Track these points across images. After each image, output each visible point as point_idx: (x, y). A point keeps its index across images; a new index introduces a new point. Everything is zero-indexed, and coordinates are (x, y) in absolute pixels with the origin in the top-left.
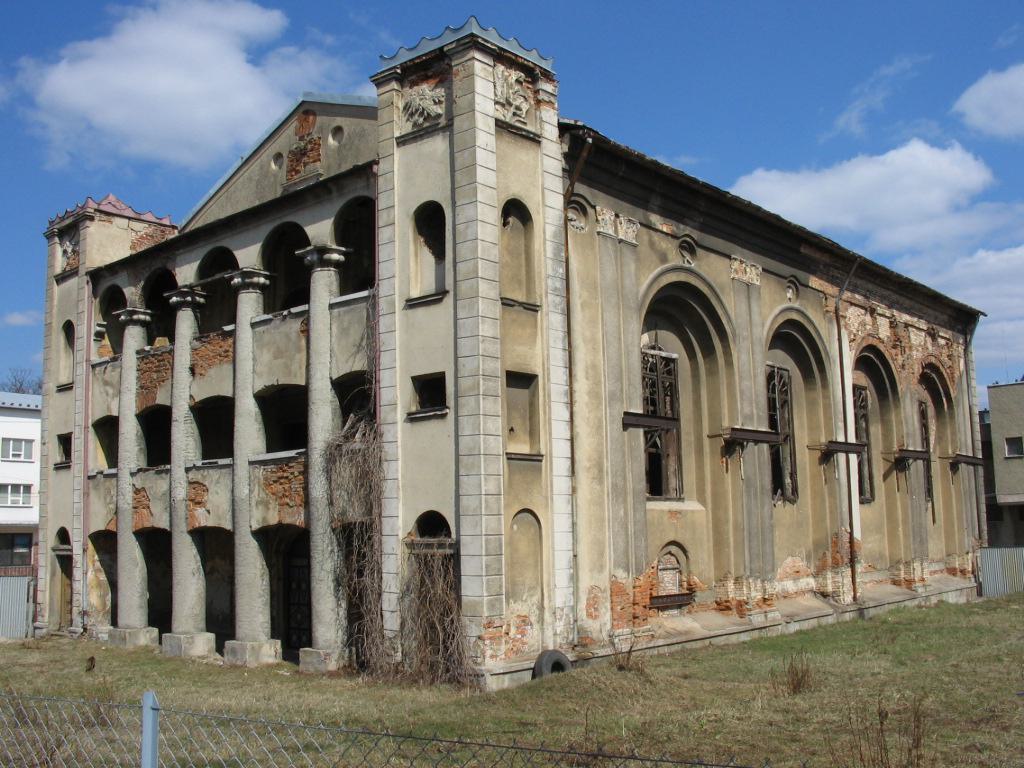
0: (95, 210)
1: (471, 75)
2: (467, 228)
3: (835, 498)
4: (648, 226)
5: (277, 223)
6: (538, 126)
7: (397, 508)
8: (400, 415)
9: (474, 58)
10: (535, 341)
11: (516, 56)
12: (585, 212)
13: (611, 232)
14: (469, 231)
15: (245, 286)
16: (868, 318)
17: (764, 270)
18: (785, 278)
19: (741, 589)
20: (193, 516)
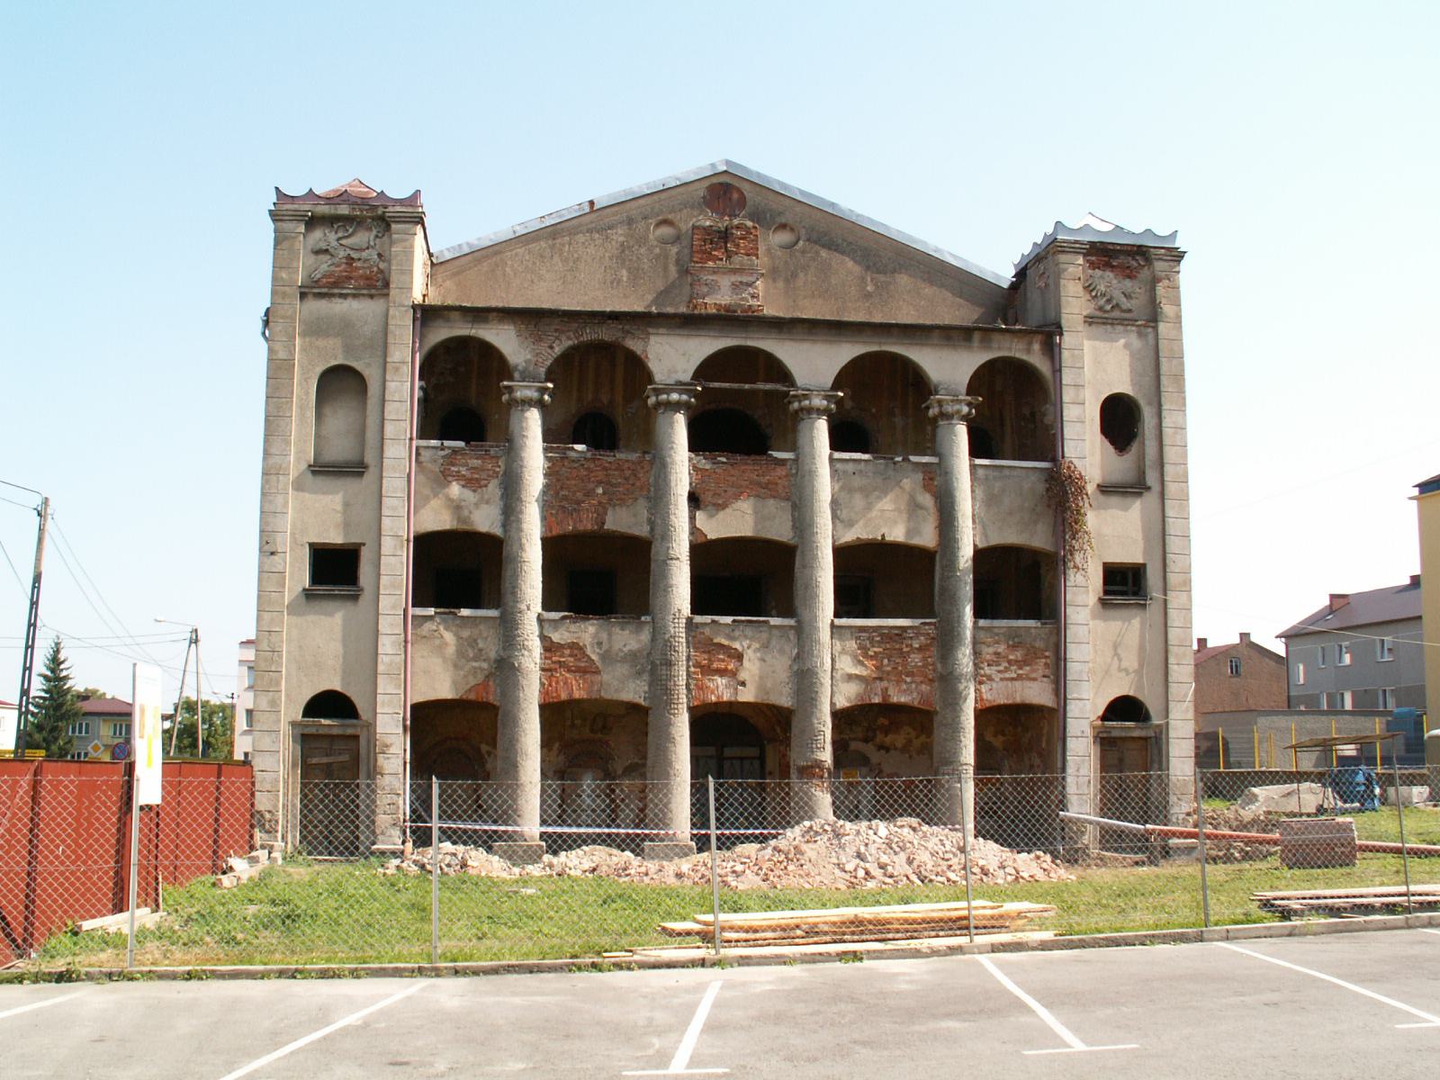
2: (1176, 433)
5: (874, 348)
14: (1178, 437)
20: (701, 688)
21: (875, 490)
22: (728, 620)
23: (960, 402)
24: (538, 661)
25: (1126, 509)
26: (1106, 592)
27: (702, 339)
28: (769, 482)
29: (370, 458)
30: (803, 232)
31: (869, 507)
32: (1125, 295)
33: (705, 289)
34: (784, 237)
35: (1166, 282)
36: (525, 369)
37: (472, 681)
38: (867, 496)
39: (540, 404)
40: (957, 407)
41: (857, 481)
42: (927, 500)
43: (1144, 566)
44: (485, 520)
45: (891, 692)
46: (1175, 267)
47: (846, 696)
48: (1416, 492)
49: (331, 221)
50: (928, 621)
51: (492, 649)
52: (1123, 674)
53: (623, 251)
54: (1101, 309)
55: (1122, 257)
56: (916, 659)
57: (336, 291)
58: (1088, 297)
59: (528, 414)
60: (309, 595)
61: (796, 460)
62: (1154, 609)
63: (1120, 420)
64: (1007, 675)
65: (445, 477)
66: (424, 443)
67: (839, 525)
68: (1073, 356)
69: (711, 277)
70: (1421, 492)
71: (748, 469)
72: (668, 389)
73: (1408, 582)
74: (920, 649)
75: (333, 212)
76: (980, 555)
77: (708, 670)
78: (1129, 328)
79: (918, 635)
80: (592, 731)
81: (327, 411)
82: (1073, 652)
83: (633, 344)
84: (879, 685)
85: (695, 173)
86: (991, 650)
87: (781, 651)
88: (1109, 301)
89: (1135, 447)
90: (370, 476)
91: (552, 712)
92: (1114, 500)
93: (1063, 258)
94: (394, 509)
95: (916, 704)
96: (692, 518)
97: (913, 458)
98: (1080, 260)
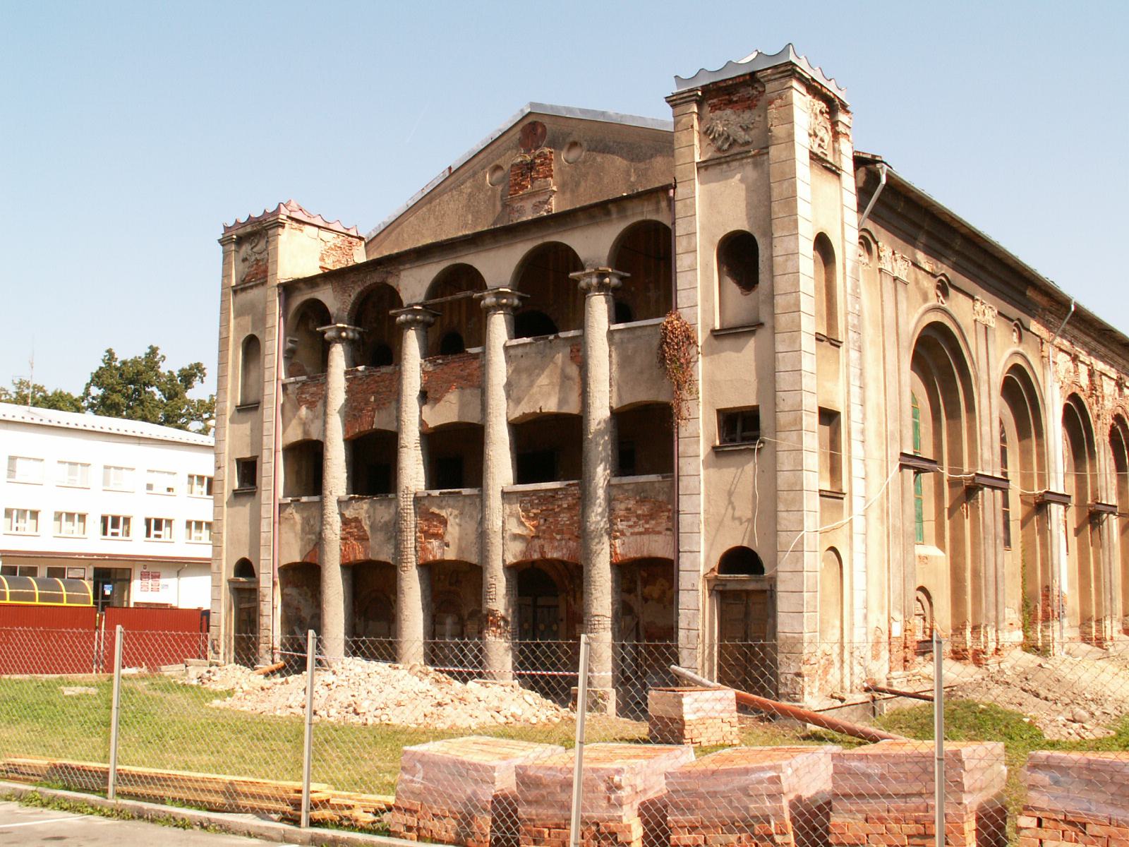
0: (288, 217)
1: (789, 105)
3: (1047, 550)
4: (915, 264)
5: (539, 242)
6: (837, 159)
7: (699, 543)
8: (703, 449)
9: (791, 87)
10: (838, 378)
11: (822, 86)
12: (869, 250)
13: (890, 270)
14: (790, 264)
15: (498, 307)
16: (1071, 365)
17: (999, 313)
18: (1012, 321)
19: (978, 638)
20: (424, 549)
24: (338, 532)
25: (739, 350)
27: (430, 266)
31: (531, 385)
32: (744, 130)
38: (530, 375)
41: (525, 363)
46: (786, 82)
47: (514, 552)
50: (571, 482)
52: (737, 523)
55: (743, 90)
61: (484, 353)
63: (741, 257)
64: (636, 530)
65: (300, 402)
68: (685, 205)
74: (570, 508)
77: (429, 535)
78: (745, 161)
79: (566, 496)
80: (451, 584)
84: (537, 542)
86: (623, 506)
87: (471, 517)
92: (727, 343)
97: (562, 335)
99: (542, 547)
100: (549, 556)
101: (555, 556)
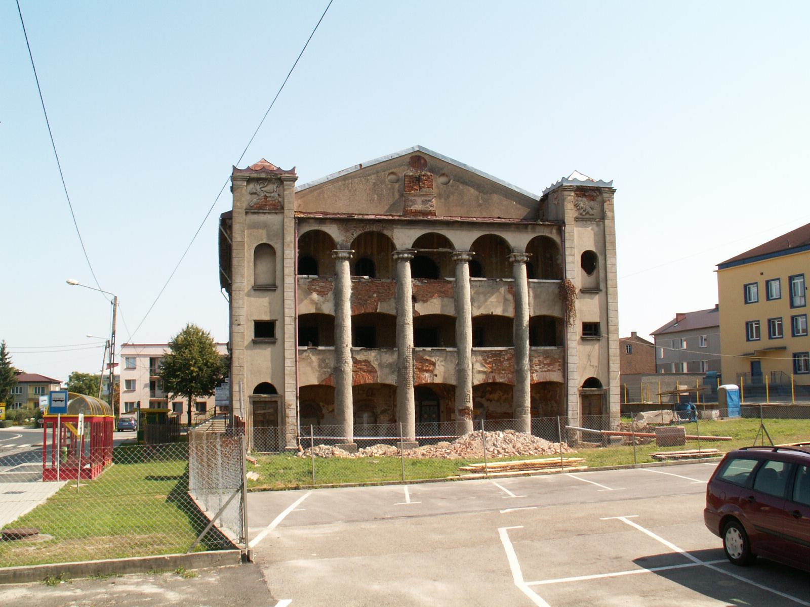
5: (488, 233)
20: (419, 378)
21: (488, 293)
22: (429, 349)
23: (523, 255)
24: (351, 368)
25: (592, 299)
26: (584, 334)
28: (445, 291)
29: (278, 283)
30: (452, 177)
31: (486, 301)
33: (411, 203)
34: (443, 179)
35: (608, 202)
36: (342, 244)
37: (324, 377)
39: (349, 259)
40: (522, 258)
41: (481, 290)
42: (510, 297)
43: (599, 323)
44: (327, 309)
45: (496, 378)
47: (479, 379)
48: (717, 268)
49: (257, 180)
51: (332, 363)
52: (592, 367)
53: (375, 187)
54: (581, 214)
56: (506, 364)
57: (261, 211)
58: (576, 209)
59: (344, 263)
60: (254, 342)
62: (603, 341)
63: (589, 261)
65: (309, 291)
66: (300, 276)
67: (474, 309)
68: (570, 235)
69: (413, 198)
70: (719, 268)
71: (435, 285)
72: (403, 252)
73: (714, 307)
75: (258, 176)
76: (531, 318)
77: (422, 370)
79: (507, 354)
81: (258, 262)
82: (571, 360)
83: (387, 232)
85: (405, 151)
86: (536, 359)
87: (451, 361)
88: (584, 211)
89: (595, 272)
90: (279, 291)
91: (356, 389)
92: (587, 295)
93: (566, 193)
94: (290, 305)
95: (506, 382)
96: (414, 307)
98: (573, 194)
99: (494, 377)
100: (498, 381)
101: (501, 381)
